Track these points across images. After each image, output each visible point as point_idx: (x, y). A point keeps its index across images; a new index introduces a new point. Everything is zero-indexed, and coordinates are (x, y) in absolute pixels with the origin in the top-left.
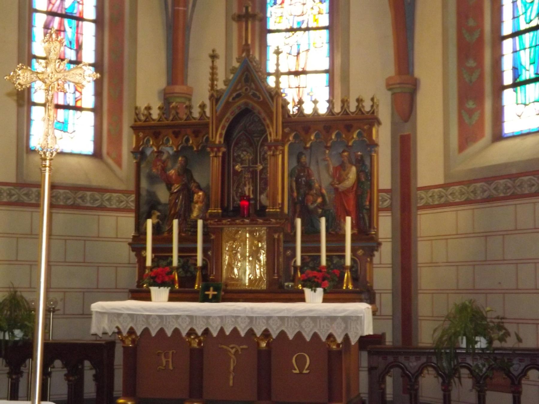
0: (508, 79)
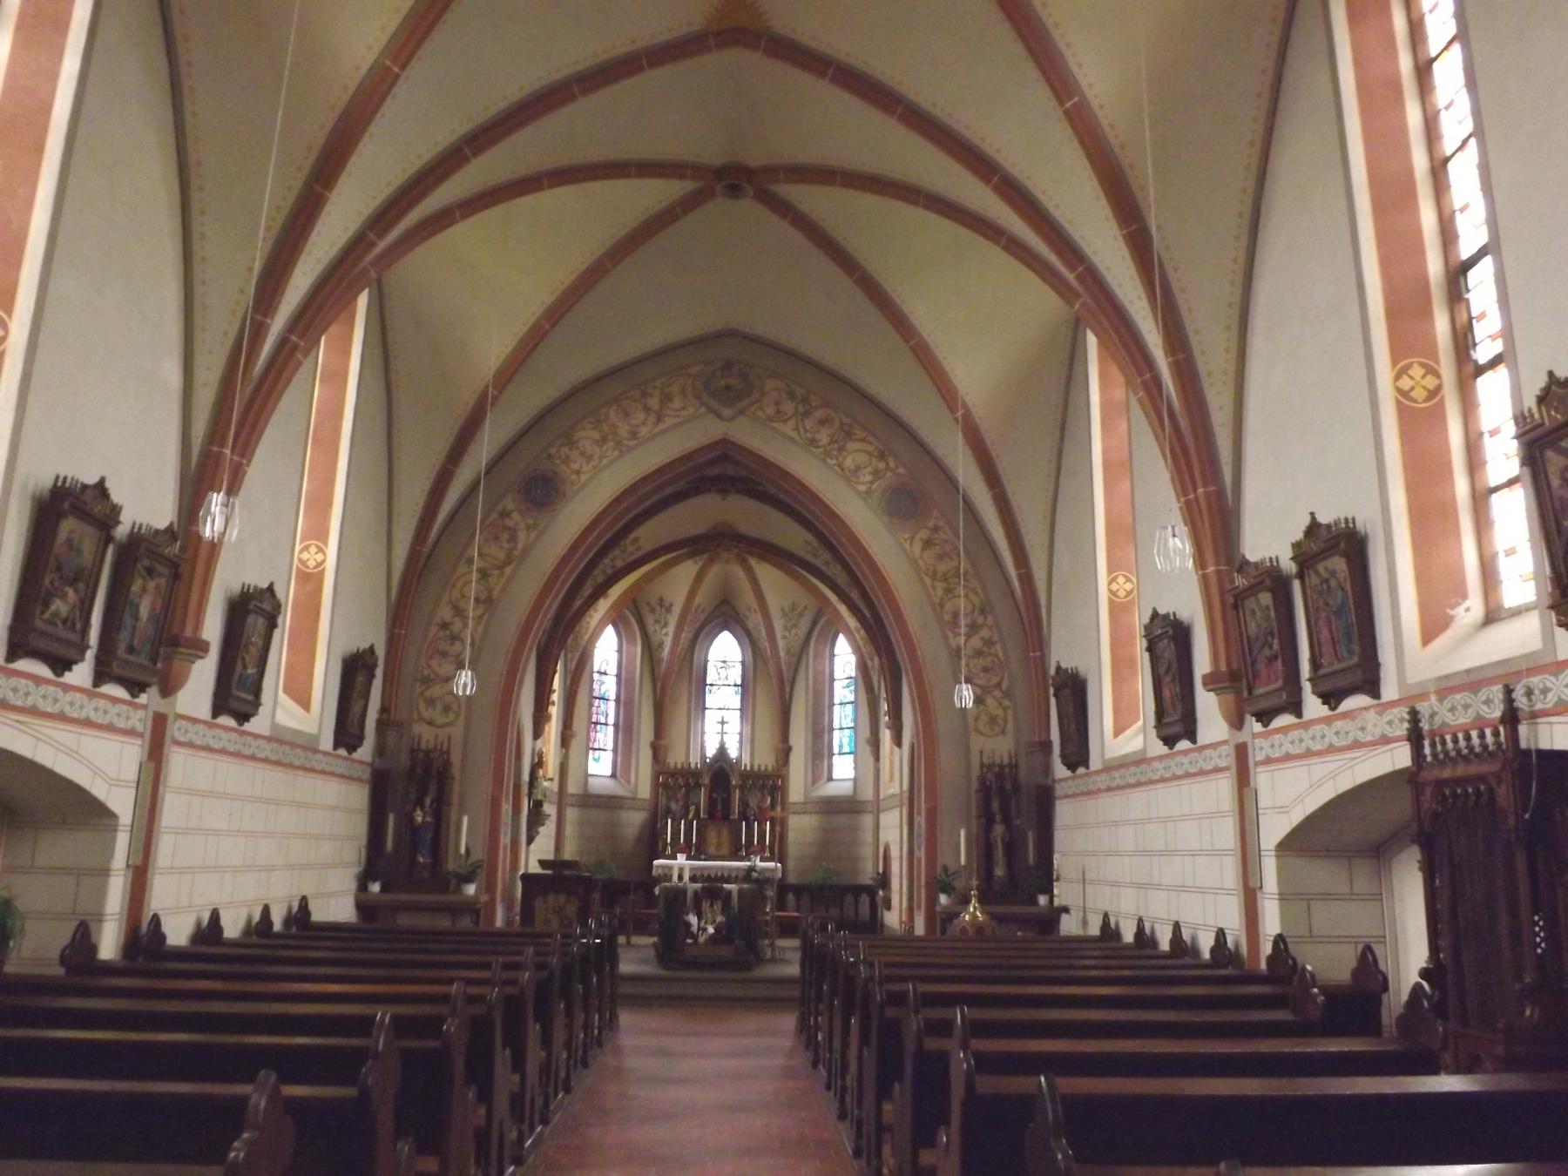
0: (836, 750)
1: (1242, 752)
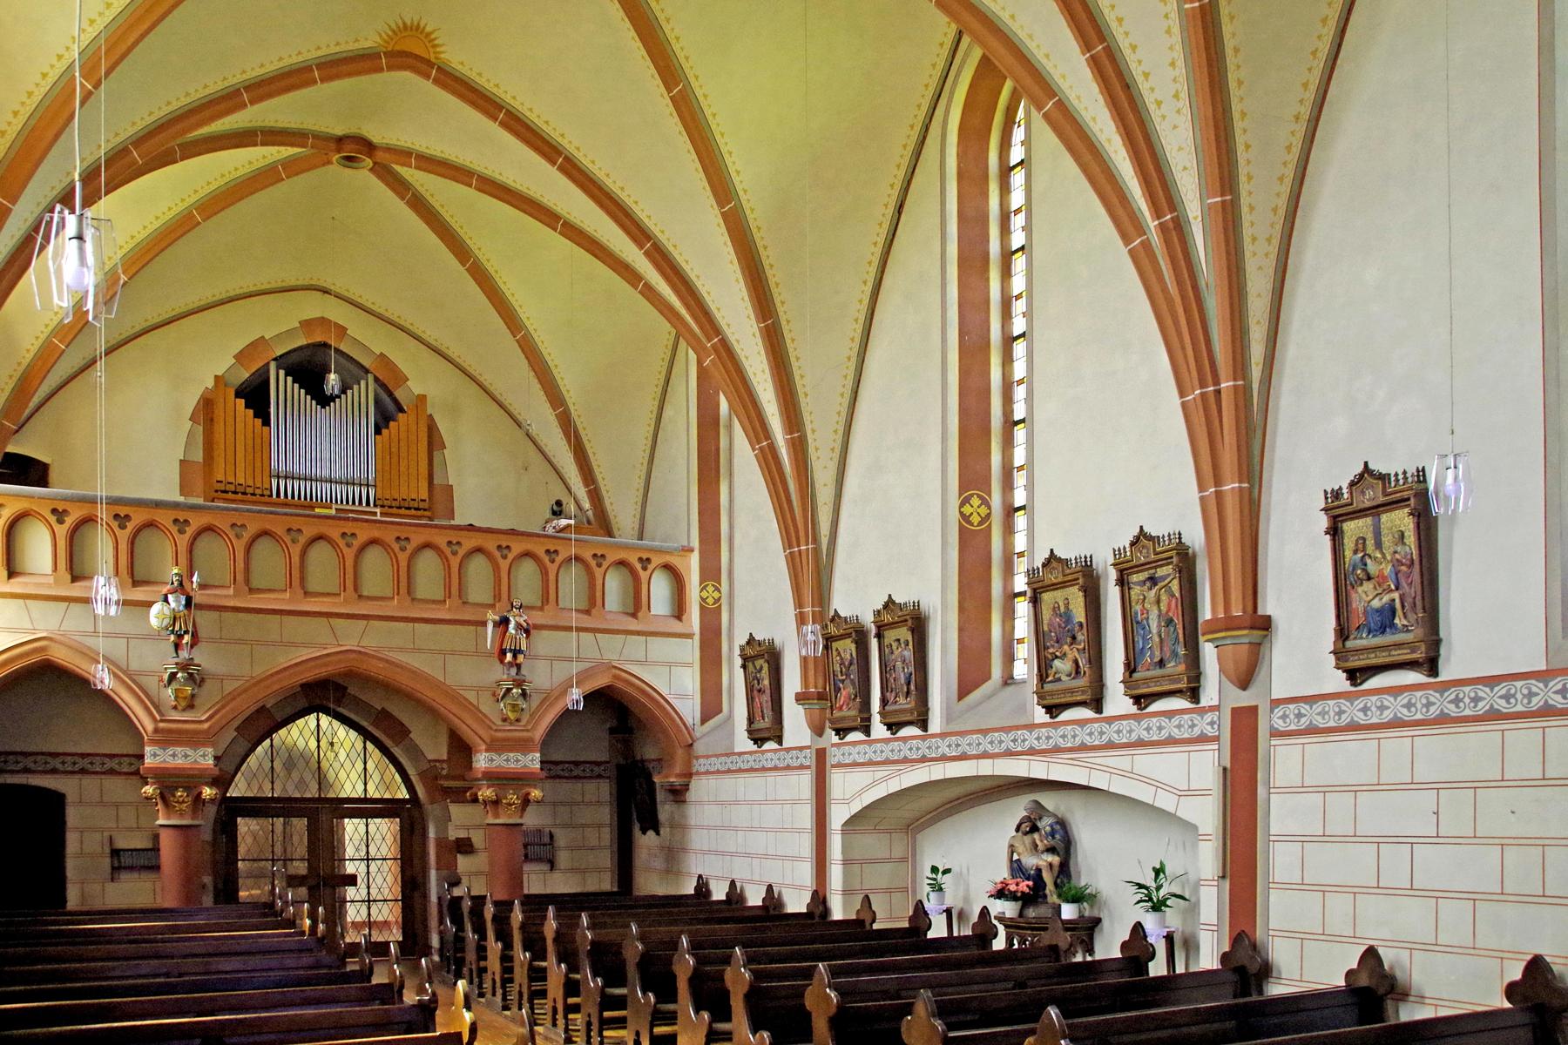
1: (821, 755)
